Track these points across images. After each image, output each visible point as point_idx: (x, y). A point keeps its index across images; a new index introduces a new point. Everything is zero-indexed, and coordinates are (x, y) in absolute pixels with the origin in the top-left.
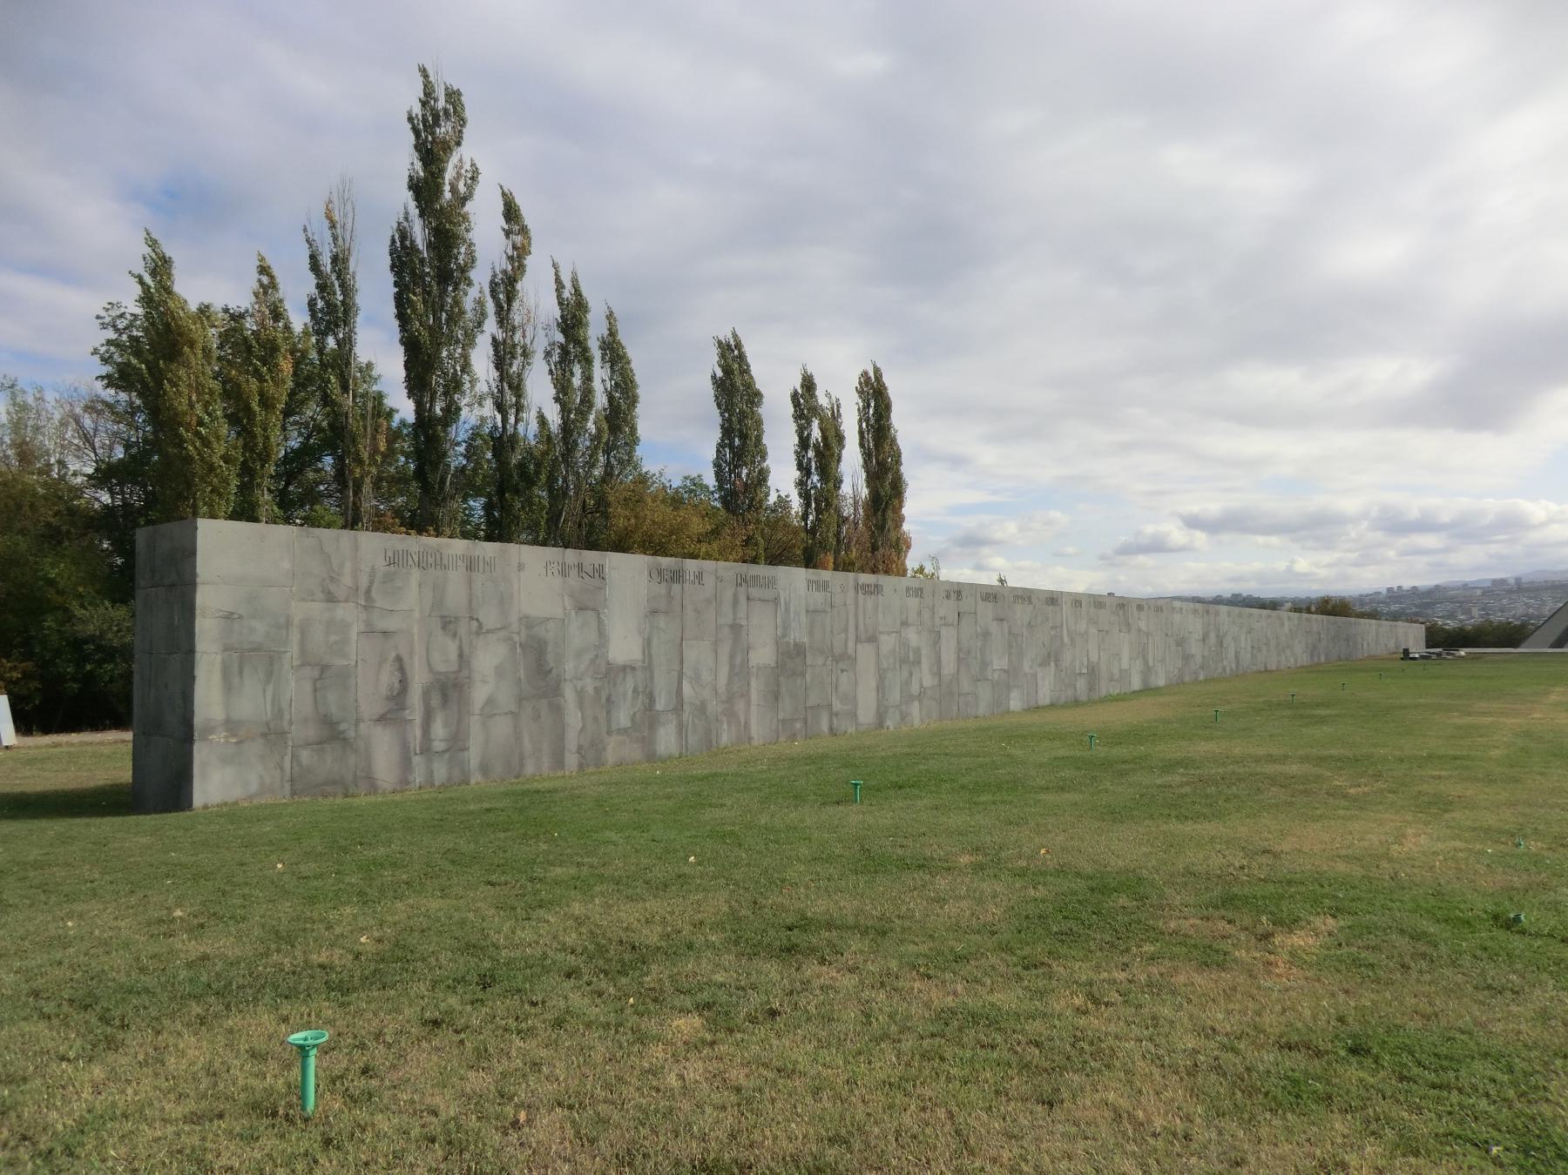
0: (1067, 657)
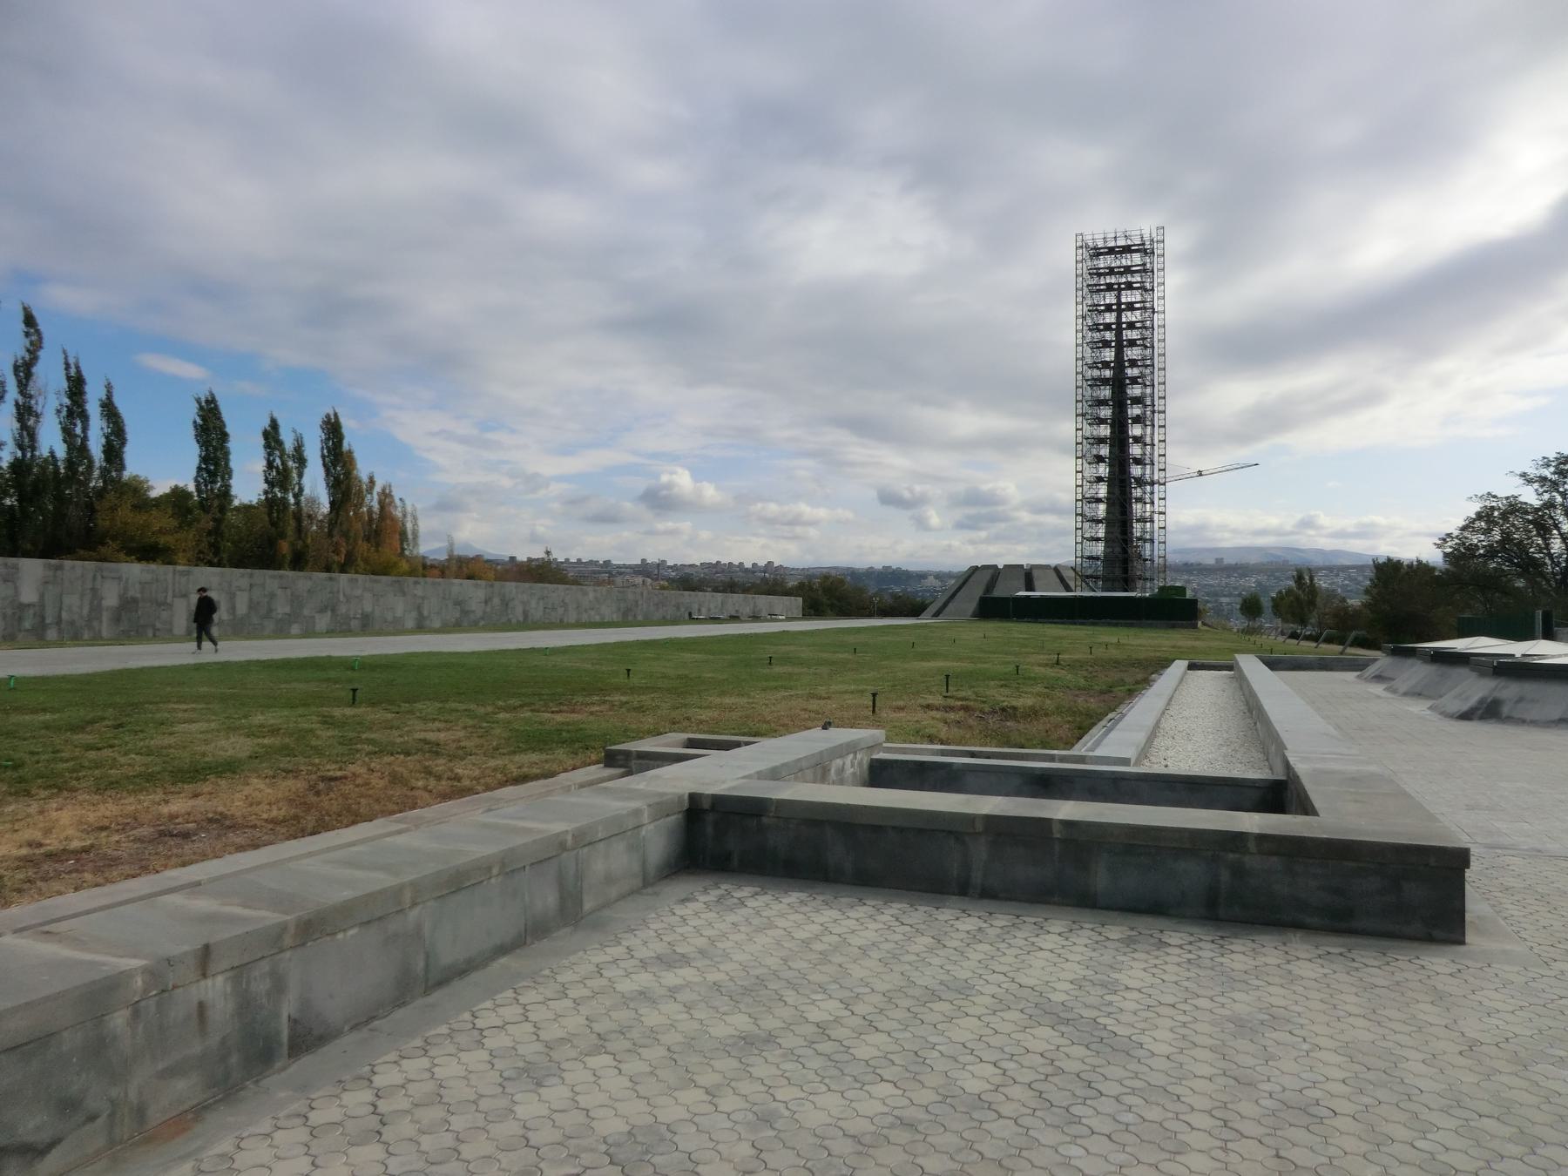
0: (343, 609)
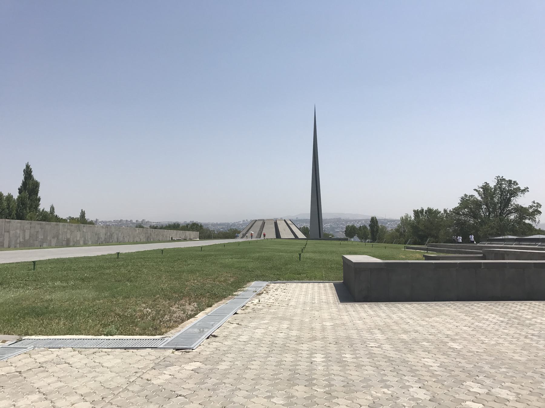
0: (60, 237)
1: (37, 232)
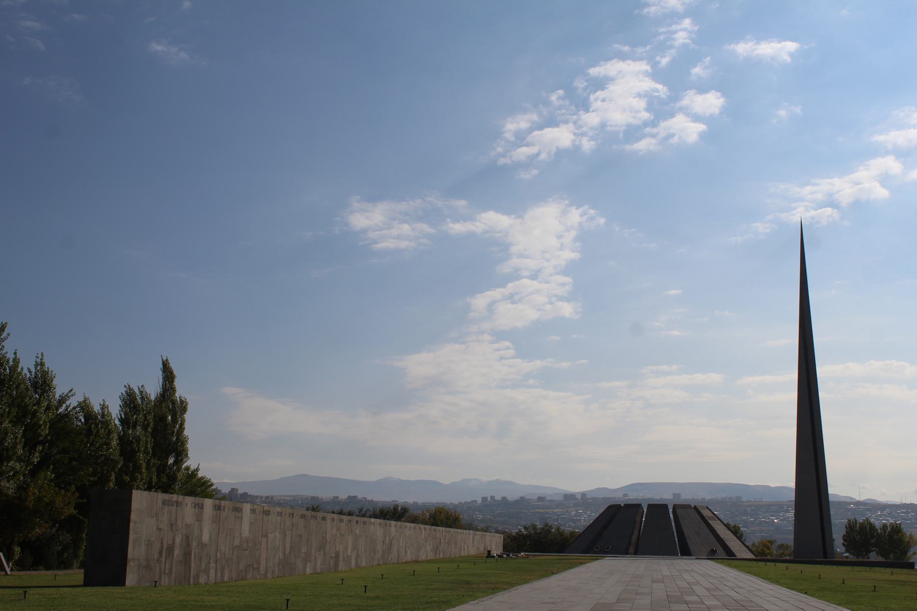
1: (300, 536)
